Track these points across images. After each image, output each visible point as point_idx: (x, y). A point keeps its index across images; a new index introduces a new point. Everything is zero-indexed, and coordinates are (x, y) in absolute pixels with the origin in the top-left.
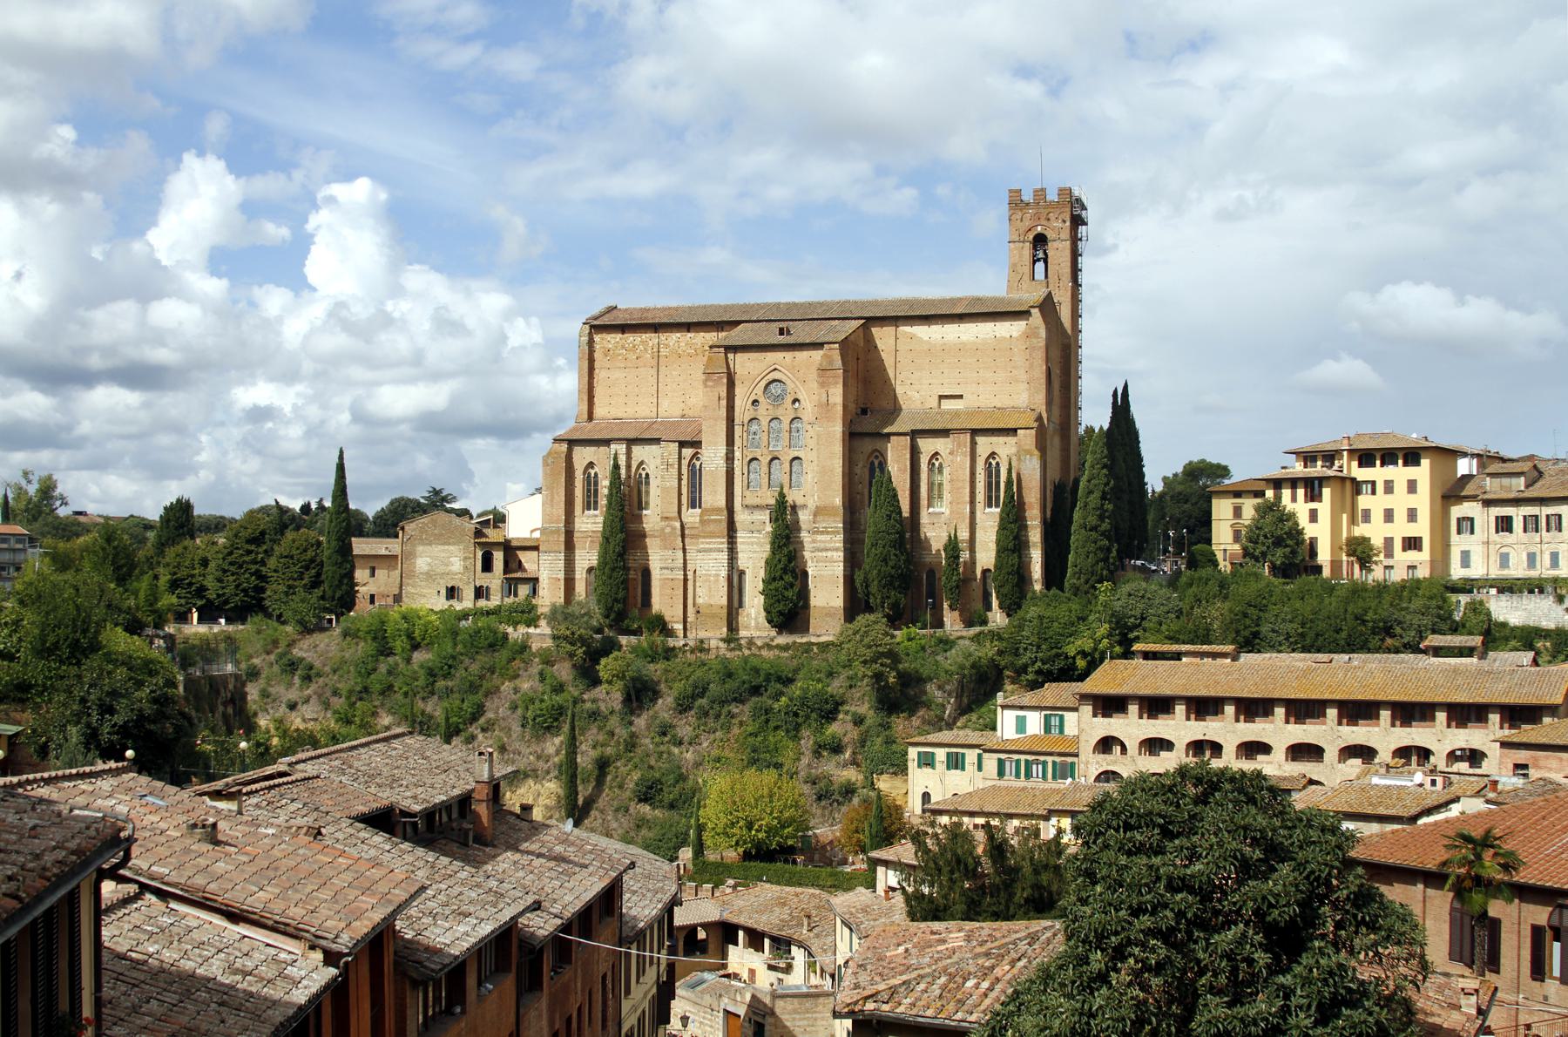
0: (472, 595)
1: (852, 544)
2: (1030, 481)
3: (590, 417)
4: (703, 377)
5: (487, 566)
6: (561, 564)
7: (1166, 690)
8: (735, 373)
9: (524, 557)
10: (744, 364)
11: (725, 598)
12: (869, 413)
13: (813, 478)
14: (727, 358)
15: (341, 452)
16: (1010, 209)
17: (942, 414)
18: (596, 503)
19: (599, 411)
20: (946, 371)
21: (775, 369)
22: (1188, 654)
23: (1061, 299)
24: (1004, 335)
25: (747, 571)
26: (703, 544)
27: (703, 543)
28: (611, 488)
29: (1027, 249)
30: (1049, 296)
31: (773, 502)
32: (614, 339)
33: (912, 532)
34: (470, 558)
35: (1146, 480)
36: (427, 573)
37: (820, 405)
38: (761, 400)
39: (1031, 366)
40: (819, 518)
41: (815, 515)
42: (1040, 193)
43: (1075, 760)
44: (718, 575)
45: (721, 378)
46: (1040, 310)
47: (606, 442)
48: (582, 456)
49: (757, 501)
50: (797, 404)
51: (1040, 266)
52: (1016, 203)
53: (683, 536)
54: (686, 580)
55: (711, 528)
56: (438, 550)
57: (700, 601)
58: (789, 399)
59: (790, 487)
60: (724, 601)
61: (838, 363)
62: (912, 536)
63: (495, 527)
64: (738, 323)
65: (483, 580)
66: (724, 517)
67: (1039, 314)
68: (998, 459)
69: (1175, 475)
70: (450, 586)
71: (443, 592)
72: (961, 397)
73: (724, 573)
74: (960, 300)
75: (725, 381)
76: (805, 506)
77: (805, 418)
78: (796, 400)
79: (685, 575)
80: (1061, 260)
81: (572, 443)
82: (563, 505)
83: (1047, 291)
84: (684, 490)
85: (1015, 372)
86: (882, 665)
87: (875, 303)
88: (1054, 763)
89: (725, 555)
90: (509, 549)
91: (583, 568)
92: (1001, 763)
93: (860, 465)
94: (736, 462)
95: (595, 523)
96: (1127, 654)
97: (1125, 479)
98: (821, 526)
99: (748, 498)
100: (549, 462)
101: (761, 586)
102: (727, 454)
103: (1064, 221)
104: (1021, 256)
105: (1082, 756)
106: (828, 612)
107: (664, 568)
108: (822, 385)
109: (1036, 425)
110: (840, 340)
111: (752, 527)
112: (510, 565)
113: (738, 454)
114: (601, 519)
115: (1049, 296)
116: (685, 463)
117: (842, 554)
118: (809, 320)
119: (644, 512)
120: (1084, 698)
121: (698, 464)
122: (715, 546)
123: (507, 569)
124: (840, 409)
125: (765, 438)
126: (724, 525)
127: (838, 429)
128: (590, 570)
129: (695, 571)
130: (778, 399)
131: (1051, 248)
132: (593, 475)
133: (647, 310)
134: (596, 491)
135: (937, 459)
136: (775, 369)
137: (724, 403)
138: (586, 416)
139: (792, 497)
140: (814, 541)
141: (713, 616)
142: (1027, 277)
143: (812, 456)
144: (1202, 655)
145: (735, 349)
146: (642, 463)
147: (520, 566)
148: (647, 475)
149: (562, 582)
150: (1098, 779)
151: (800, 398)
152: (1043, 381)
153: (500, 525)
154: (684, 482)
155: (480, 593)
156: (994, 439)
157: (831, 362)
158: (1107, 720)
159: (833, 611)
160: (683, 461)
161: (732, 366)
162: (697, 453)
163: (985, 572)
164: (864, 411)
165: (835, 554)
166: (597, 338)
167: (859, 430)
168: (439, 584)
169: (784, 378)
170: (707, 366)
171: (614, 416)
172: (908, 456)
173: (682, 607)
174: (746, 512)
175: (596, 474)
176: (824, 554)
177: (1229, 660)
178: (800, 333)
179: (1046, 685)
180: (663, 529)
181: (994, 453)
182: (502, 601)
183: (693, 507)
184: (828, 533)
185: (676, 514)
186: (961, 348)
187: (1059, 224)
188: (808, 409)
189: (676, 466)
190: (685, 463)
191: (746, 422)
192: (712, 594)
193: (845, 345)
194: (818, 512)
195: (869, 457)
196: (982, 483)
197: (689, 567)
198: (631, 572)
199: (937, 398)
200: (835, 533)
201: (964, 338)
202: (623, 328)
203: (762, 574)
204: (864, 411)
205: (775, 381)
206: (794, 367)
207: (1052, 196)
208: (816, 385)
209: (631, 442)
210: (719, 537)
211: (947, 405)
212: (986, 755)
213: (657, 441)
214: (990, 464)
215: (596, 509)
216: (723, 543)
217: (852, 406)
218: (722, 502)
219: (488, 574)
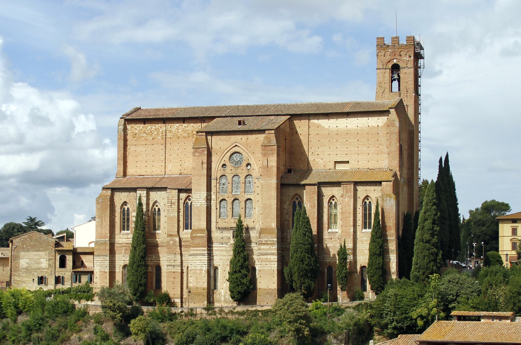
0: (53, 282)
1: (282, 251)
2: (390, 213)
3: (125, 175)
5: (63, 264)
6: (107, 263)
8: (212, 148)
9: (85, 259)
10: (217, 142)
11: (206, 283)
12: (293, 172)
13: (259, 211)
14: (207, 139)
16: (378, 49)
18: (128, 226)
19: (130, 171)
20: (339, 147)
21: (236, 146)
23: (408, 104)
24: (374, 125)
25: (219, 267)
27: (192, 250)
28: (137, 217)
29: (388, 72)
30: (401, 102)
31: (234, 225)
33: (318, 243)
34: (52, 259)
35: (459, 212)
36: (26, 268)
37: (263, 167)
38: (228, 164)
39: (390, 143)
40: (262, 236)
41: (260, 234)
42: (395, 40)
44: (201, 270)
45: (203, 151)
46: (396, 110)
47: (134, 190)
48: (120, 198)
49: (225, 225)
50: (249, 167)
51: (395, 83)
52: (381, 45)
53: (181, 246)
54: (182, 273)
55: (197, 241)
56: (32, 254)
57: (190, 285)
58: (244, 164)
59: (245, 217)
60: (205, 285)
61: (274, 142)
62: (318, 246)
63: (68, 240)
64: (213, 118)
65: (60, 272)
66: (205, 234)
67: (395, 113)
68: (370, 200)
69: (477, 209)
70: (40, 276)
71: (36, 280)
72: (348, 162)
73: (205, 268)
74: (347, 104)
75: (206, 152)
76: (254, 228)
78: (248, 164)
79: (182, 270)
80: (408, 79)
81: (114, 190)
82: (108, 228)
83: (400, 98)
84: (181, 219)
85: (380, 147)
86: (300, 324)
87: (296, 106)
89: (206, 258)
90: (76, 254)
91: (120, 265)
93: (287, 203)
94: (212, 201)
95: (128, 238)
96: (448, 317)
97: (447, 212)
98: (264, 240)
99: (219, 223)
100: (100, 201)
101: (227, 276)
102: (207, 197)
103: (410, 57)
104: (384, 77)
106: (268, 292)
107: (171, 266)
108: (264, 155)
109: (393, 179)
110: (275, 128)
111: (222, 241)
112: (76, 263)
113: (213, 197)
114: (131, 236)
115: (401, 102)
116: (182, 202)
117: (276, 257)
118: (256, 116)
119: (157, 232)
121: (189, 202)
122: (200, 252)
123: (74, 266)
124: (275, 169)
126: (206, 239)
127: (273, 181)
128: (125, 267)
129: (188, 267)
130: (238, 164)
132: (126, 209)
133: (159, 110)
134: (128, 219)
135: (333, 200)
136: (236, 146)
137: (205, 166)
138: (122, 174)
139: (246, 222)
140: (259, 249)
141: (199, 294)
142: (387, 90)
143: (259, 198)
144: (493, 318)
146: (156, 202)
147: (82, 264)
148: (159, 209)
149: (108, 274)
151: (251, 162)
152: (397, 153)
153: (70, 239)
154: (181, 214)
155: (58, 280)
156: (368, 188)
157: (270, 141)
159: (271, 291)
160: (180, 201)
161: (210, 144)
162: (189, 196)
163: (362, 268)
164: (290, 171)
165: (272, 257)
166: (129, 127)
167: (287, 182)
168: (33, 275)
169: (241, 151)
170: (195, 144)
171: (139, 174)
172: (316, 198)
173: (180, 289)
174: (219, 231)
175: (128, 209)
176: (266, 257)
177: (509, 321)
178: (251, 124)
179: (399, 336)
180: (168, 242)
181: (367, 196)
182: (72, 285)
183: (187, 228)
184: (268, 244)
185: (177, 233)
186: (348, 133)
188: (256, 169)
189: (177, 204)
190: (182, 202)
191: (218, 177)
193: (278, 131)
194: (262, 231)
195: (292, 199)
196: (361, 214)
197: (184, 265)
198: (149, 268)
199: (333, 163)
200: (274, 244)
201: (350, 127)
202: (145, 121)
203: (228, 269)
204: (290, 171)
206: (247, 144)
208: (260, 155)
209: (149, 189)
210: (202, 247)
211: (339, 167)
213: (165, 189)
214: (366, 203)
215: (128, 230)
216: (204, 250)
217: (282, 168)
218: (204, 225)
219: (63, 269)
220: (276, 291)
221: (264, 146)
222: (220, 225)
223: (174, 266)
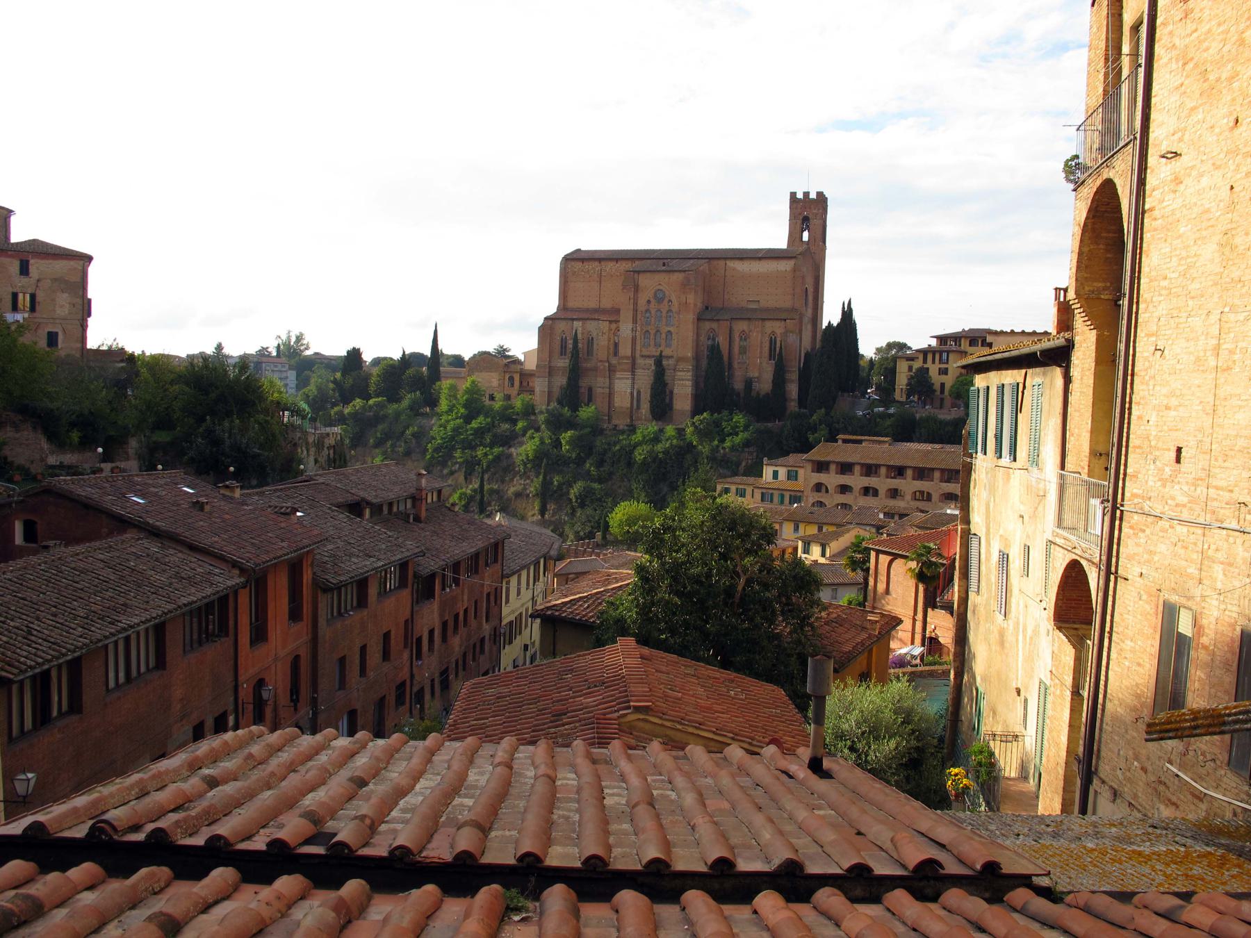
7: (850, 460)
8: (638, 286)
10: (646, 281)
17: (748, 310)
18: (565, 352)
22: (865, 440)
32: (578, 265)
38: (652, 300)
40: (679, 363)
42: (806, 194)
43: (801, 494)
47: (573, 320)
57: (616, 405)
60: (629, 405)
73: (629, 391)
77: (674, 310)
88: (790, 496)
89: (629, 382)
92: (763, 494)
105: (805, 494)
114: (567, 361)
125: (653, 320)
134: (566, 347)
137: (632, 301)
142: (798, 240)
144: (874, 441)
145: (639, 272)
150: (813, 505)
158: (818, 474)
169: (664, 289)
175: (566, 338)
177: (887, 445)
178: (674, 264)
200: (688, 371)
201: (761, 270)
205: (661, 290)
207: (813, 196)
212: (756, 490)
215: (565, 355)
217: (699, 305)
218: (629, 353)
220: (689, 413)
222: (644, 353)
223: (603, 388)
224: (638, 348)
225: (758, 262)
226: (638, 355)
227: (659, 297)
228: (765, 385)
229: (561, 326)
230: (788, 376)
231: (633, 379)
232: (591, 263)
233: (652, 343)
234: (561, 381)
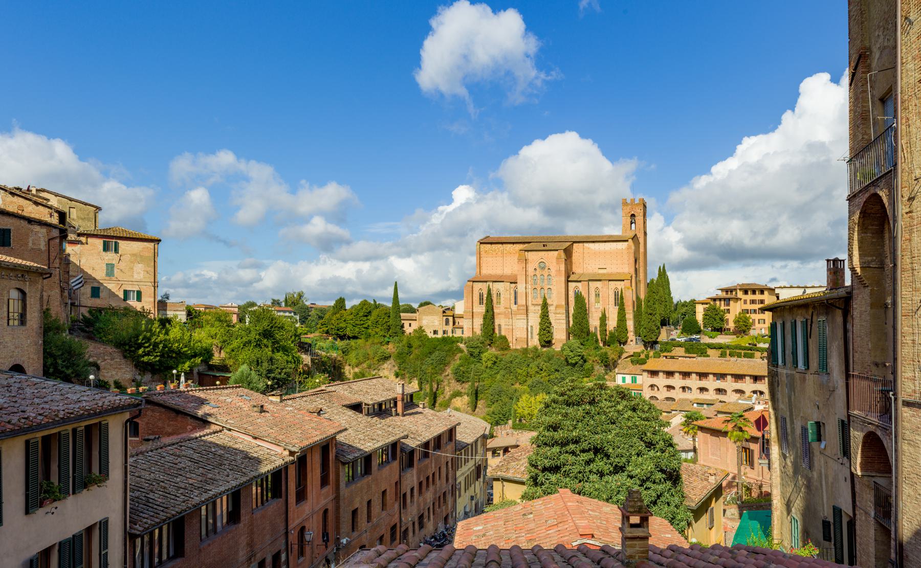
4: (517, 260)
7: (671, 369)
10: (530, 255)
15: (396, 283)
26: (518, 317)
29: (629, 220)
31: (541, 303)
41: (556, 308)
42: (633, 201)
47: (486, 282)
51: (633, 225)
76: (552, 305)
98: (558, 311)
108: (558, 264)
120: (644, 371)
124: (564, 272)
126: (525, 311)
127: (563, 279)
130: (543, 268)
131: (636, 218)
133: (500, 238)
134: (483, 299)
143: (555, 288)
166: (482, 246)
180: (505, 312)
187: (639, 211)
188: (553, 272)
192: (520, 334)
194: (557, 307)
200: (563, 314)
202: (491, 243)
207: (637, 202)
213: (503, 282)
221: (557, 259)
224: (530, 299)
225: (604, 244)
226: (530, 303)
227: (542, 266)
228: (612, 324)
229: (477, 286)
230: (627, 316)
231: (527, 319)
232: (496, 245)
233: (539, 296)
234: (479, 322)
